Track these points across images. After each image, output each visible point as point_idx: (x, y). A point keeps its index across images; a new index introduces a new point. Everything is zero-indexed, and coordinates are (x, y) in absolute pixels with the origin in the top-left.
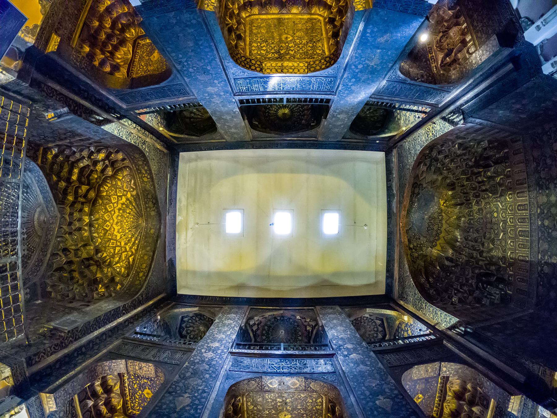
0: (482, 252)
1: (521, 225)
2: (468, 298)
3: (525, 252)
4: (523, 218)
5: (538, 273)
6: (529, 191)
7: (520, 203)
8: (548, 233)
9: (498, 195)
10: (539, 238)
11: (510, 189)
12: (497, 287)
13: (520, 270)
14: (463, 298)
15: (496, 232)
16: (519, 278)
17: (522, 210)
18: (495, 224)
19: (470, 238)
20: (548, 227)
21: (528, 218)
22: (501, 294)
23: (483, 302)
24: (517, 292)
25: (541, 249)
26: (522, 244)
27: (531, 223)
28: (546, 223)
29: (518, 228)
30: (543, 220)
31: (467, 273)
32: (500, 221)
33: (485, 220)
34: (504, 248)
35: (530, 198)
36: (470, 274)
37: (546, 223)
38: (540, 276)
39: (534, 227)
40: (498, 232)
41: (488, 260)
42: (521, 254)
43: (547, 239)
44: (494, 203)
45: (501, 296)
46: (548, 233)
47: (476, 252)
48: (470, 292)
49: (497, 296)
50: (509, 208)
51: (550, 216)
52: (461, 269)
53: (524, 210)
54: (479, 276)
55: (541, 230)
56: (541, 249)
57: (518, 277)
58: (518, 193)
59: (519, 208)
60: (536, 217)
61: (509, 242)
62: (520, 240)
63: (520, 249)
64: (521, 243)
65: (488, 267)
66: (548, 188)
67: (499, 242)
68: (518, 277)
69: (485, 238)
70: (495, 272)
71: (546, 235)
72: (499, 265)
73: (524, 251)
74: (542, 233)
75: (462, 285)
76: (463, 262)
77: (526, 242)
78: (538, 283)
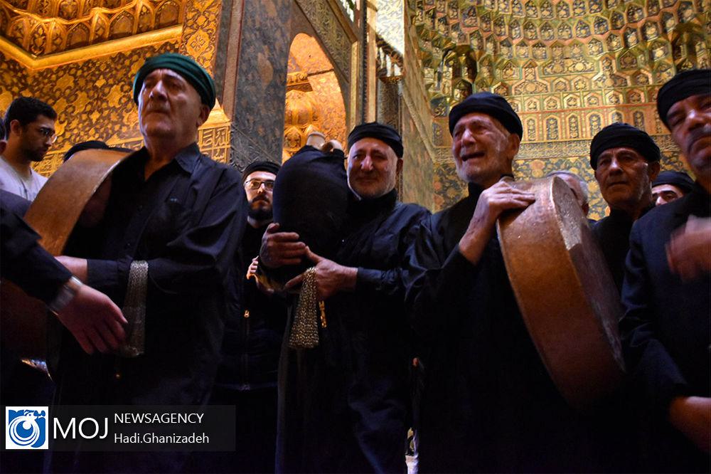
0: (510, 46)
1: (565, 122)
2: (426, 40)
4: (577, 126)
9: (615, 72)
10: (547, 159)
11: (628, 99)
12: (454, 86)
14: (424, 30)
15: (549, 70)
17: (591, 125)
18: (563, 66)
19: (531, 12)
21: (578, 136)
22: (445, 97)
23: (426, 72)
25: (531, 164)
26: (534, 125)
27: (570, 142)
29: (560, 117)
30: (577, 167)
31: (468, 21)
32: (568, 77)
33: (567, 42)
34: (522, 90)
36: (467, 31)
39: (564, 148)
40: (549, 74)
41: (496, 60)
44: (600, 63)
45: (442, 98)
47: (507, 33)
48: (437, 40)
49: (440, 92)
50: (593, 96)
52: (472, 7)
53: (591, 129)
54: (468, 50)
55: (562, 162)
56: (531, 164)
58: (618, 114)
59: (594, 119)
61: (535, 100)
62: (541, 123)
64: (536, 125)
65: (486, 62)
67: (531, 77)
69: (534, 46)
70: (477, 80)
72: (491, 83)
74: (556, 164)
75: (445, 21)
76: (486, 8)
77: (539, 135)
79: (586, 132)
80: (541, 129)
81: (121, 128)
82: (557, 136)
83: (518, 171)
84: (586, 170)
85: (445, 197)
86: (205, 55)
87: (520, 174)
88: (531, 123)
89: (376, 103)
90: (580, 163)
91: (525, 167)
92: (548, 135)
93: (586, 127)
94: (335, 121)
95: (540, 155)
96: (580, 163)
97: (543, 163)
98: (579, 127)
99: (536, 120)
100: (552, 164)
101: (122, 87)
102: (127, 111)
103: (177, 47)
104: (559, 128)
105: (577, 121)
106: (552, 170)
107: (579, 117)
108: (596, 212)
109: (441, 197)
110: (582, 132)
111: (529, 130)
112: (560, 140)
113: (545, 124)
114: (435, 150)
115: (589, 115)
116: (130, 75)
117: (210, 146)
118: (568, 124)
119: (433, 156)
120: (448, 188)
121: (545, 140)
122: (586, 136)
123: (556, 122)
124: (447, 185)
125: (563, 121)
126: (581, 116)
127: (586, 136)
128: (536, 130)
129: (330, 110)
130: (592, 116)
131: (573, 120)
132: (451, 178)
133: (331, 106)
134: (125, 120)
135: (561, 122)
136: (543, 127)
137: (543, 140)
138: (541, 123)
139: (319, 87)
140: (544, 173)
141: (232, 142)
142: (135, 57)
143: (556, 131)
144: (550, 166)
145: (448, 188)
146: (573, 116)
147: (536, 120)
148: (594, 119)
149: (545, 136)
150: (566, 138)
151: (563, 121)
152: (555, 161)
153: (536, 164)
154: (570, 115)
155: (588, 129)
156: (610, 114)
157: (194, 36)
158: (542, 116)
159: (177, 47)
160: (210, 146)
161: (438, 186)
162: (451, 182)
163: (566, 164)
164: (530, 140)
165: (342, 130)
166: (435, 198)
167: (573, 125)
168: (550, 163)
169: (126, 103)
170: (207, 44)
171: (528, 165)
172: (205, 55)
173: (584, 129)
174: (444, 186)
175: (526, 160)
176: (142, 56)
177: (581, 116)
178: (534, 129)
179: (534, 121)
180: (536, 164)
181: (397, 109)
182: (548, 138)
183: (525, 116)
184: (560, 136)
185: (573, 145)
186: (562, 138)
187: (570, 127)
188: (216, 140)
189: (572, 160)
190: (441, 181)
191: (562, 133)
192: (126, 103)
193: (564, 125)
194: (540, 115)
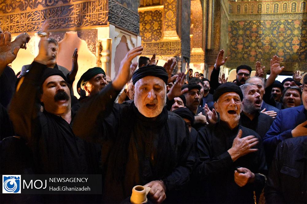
1: (282, 6)
3: (264, 10)
5: (252, 21)
6: (304, 13)
7: (297, 5)
8: (276, 28)
10: (273, 21)
13: (252, 7)
16: (247, 6)
17: (292, 7)
20: (279, 27)
24: (238, 5)
26: (269, 7)
27: (282, 14)
28: (282, 26)
29: (280, 3)
35: (299, 14)
37: (282, 26)
38: (250, 22)
42: (262, 6)
43: (272, 27)
46: (276, 28)
51: (285, 30)
53: (292, 9)
55: (278, 22)
56: (266, 22)
57: (248, 5)
60: (286, 19)
63: (266, 5)
64: (270, 6)
66: (303, 29)
68: (248, 5)
71: (275, 26)
73: (265, 9)
78: (246, 21)
79: (290, 10)
80: (272, 8)
81: (144, 38)
82: (278, 11)
83: (260, 25)
84: (287, 25)
85: (232, 34)
86: (173, 20)
87: (262, 26)
88: (268, 5)
89: (212, 7)
90: (285, 23)
91: (263, 23)
92: (274, 11)
93: (290, 8)
94: (198, 16)
95: (270, 19)
96: (285, 23)
97: (271, 22)
98: (287, 8)
99: (270, 4)
100: (274, 23)
101: (142, 24)
102: (146, 33)
103: (160, 12)
104: (279, 8)
105: (286, 5)
106: (274, 25)
107: (287, 4)
108: (288, 42)
109: (231, 34)
110: (288, 10)
111: (267, 8)
112: (278, 13)
113: (273, 6)
114: (229, 15)
115: (292, 3)
116: (144, 20)
117: (175, 47)
118: (283, 7)
119: (228, 18)
120: (234, 30)
121: (273, 13)
122: (289, 12)
123: (278, 6)
124: (233, 29)
125: (281, 5)
126: (288, 3)
127: (289, 12)
128: (270, 8)
129: (196, 12)
130: (293, 3)
131: (285, 5)
132: (235, 26)
133: (197, 10)
134: (145, 36)
135: (280, 5)
136: (272, 7)
137: (272, 12)
138: (272, 6)
139: (193, 4)
140: (271, 26)
141: (181, 47)
142: (146, 14)
143: (278, 9)
144: (273, 23)
145: (234, 30)
146: (285, 3)
147: (270, 4)
148: (294, 4)
149: (273, 11)
150: (281, 12)
151: (281, 5)
152: (275, 21)
153: (268, 22)
154: (284, 3)
155: (291, 9)
156: (301, 2)
157: (168, 12)
158: (273, 3)
159: (160, 12)
160: (175, 47)
161: (230, 29)
162: (235, 28)
163: (279, 23)
164: (267, 13)
165: (200, 19)
166: (229, 34)
167: (285, 7)
168: (273, 22)
169: (145, 30)
170: (173, 15)
171: (264, 23)
172: (173, 20)
173: (289, 9)
174: (232, 30)
175: (264, 21)
176: (148, 13)
177: (288, 3)
178: (269, 8)
179: (269, 5)
180: (268, 22)
181: (220, 9)
182: (274, 12)
183: (266, 2)
184: (279, 11)
185: (283, 15)
186: (280, 12)
187: (283, 7)
188: (177, 46)
189: (282, 21)
190: (231, 27)
191: (280, 11)
192: (145, 30)
193: (281, 6)
194: (272, 2)
